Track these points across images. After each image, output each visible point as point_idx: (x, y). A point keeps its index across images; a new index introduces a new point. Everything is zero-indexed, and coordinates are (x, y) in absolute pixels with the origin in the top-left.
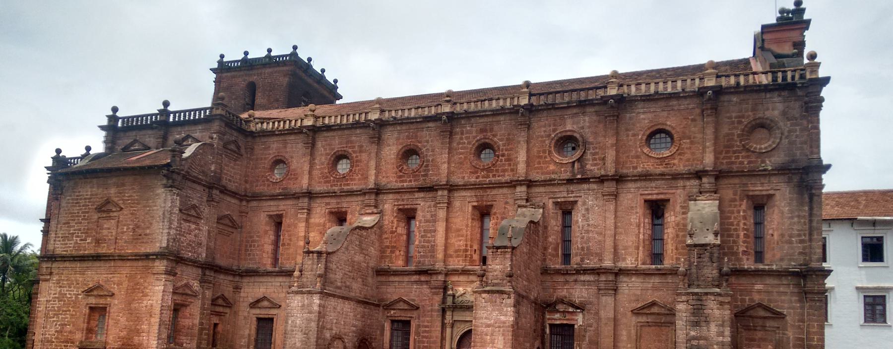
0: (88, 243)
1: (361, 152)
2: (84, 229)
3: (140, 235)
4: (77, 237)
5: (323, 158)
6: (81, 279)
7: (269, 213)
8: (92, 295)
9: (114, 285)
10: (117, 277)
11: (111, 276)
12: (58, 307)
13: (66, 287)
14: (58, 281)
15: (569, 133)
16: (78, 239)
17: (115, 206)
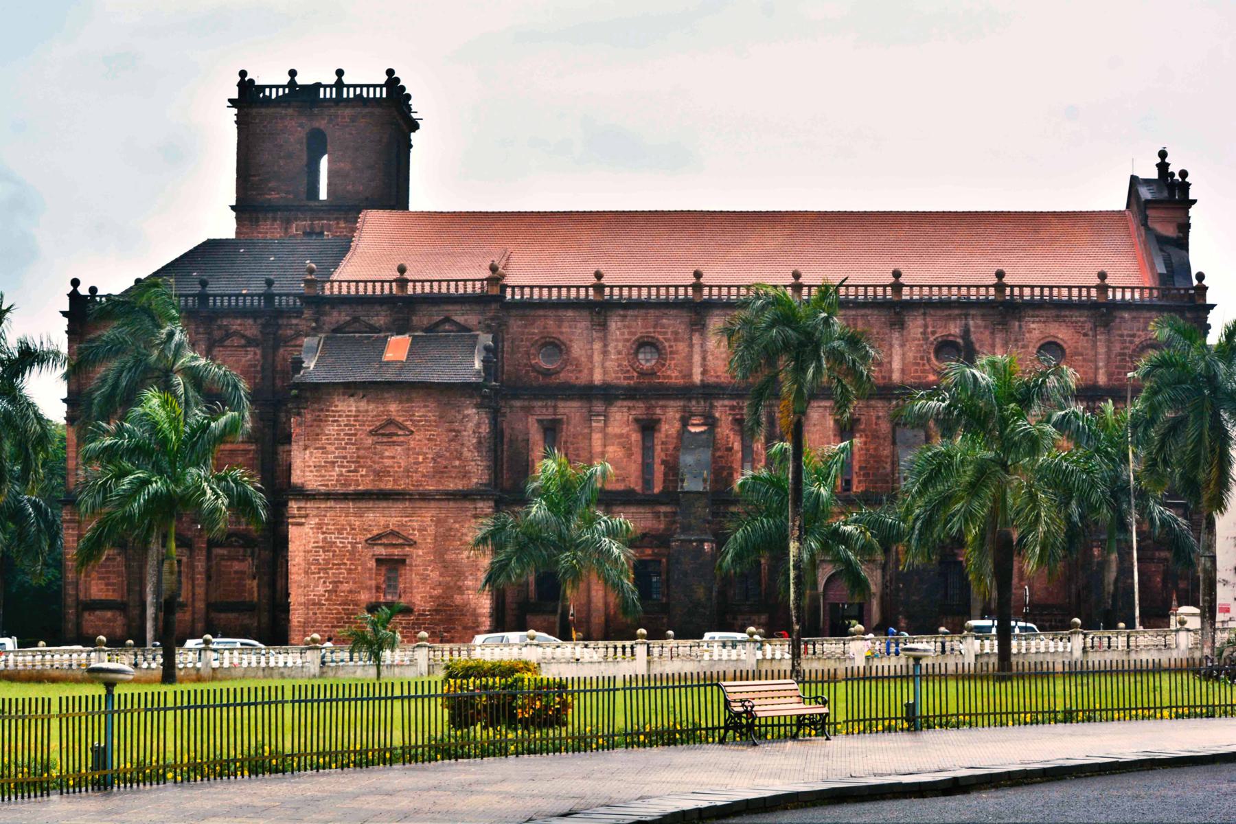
0: (362, 476)
1: (676, 340)
2: (352, 457)
3: (446, 467)
4: (343, 467)
5: (620, 345)
6: (357, 523)
7: (540, 417)
8: (381, 544)
9: (414, 530)
10: (417, 521)
11: (407, 519)
12: (324, 560)
13: (333, 533)
14: (319, 526)
15: (951, 338)
16: (344, 470)
17: (400, 428)
